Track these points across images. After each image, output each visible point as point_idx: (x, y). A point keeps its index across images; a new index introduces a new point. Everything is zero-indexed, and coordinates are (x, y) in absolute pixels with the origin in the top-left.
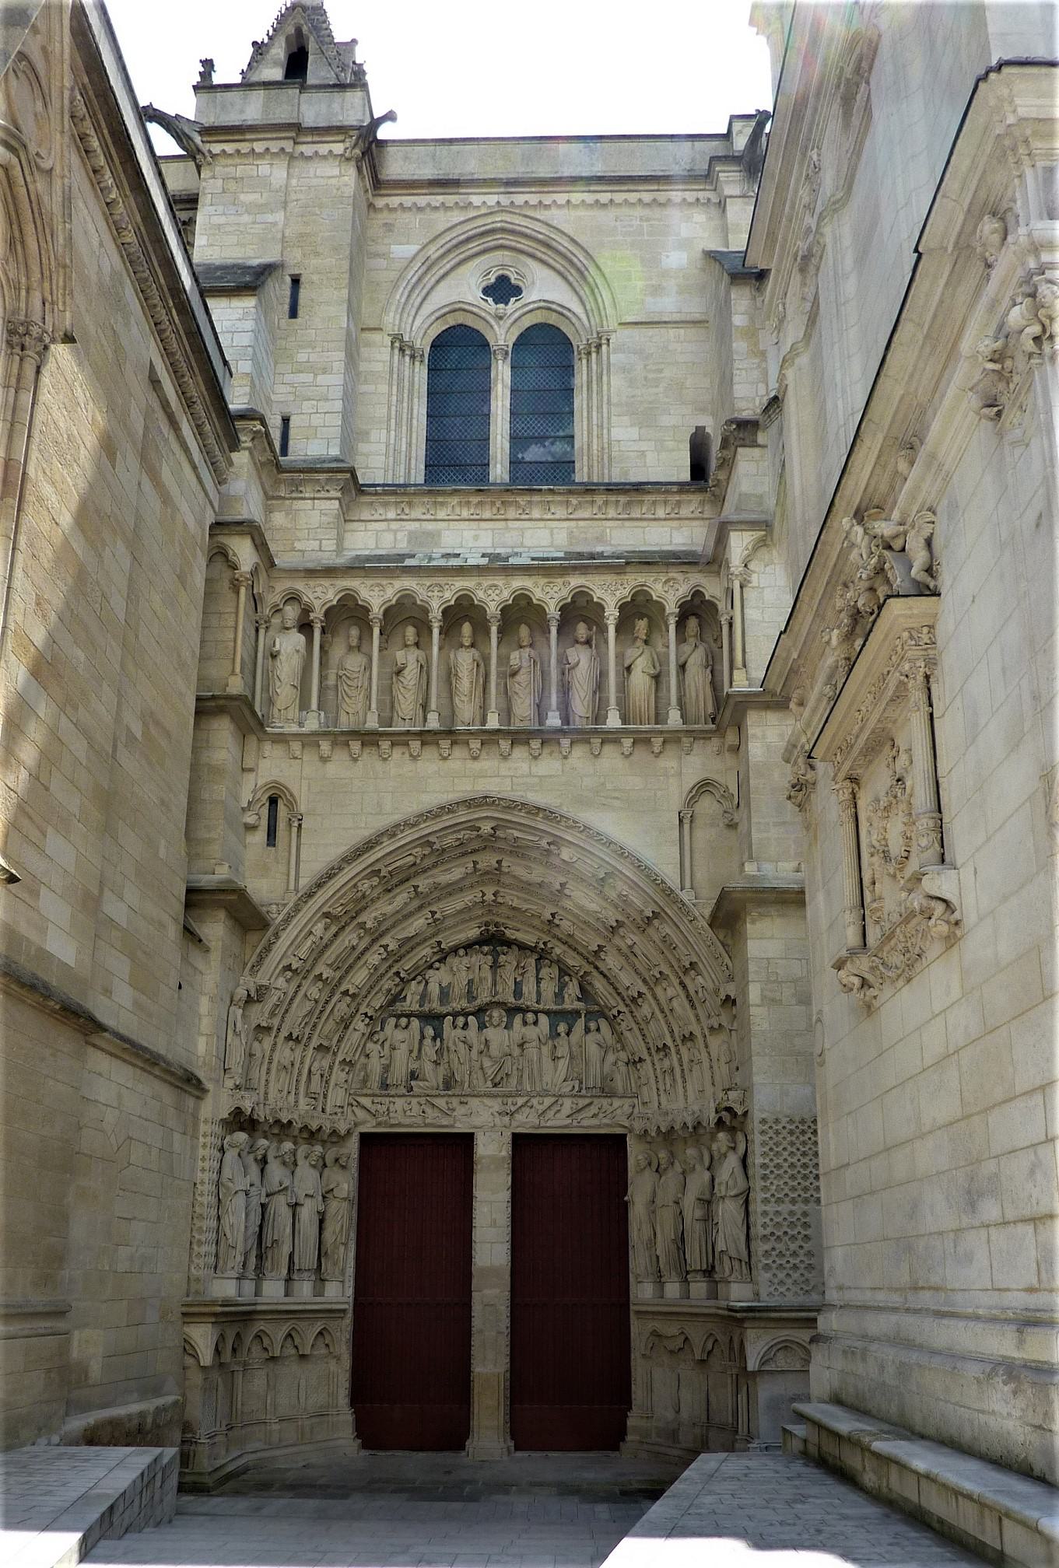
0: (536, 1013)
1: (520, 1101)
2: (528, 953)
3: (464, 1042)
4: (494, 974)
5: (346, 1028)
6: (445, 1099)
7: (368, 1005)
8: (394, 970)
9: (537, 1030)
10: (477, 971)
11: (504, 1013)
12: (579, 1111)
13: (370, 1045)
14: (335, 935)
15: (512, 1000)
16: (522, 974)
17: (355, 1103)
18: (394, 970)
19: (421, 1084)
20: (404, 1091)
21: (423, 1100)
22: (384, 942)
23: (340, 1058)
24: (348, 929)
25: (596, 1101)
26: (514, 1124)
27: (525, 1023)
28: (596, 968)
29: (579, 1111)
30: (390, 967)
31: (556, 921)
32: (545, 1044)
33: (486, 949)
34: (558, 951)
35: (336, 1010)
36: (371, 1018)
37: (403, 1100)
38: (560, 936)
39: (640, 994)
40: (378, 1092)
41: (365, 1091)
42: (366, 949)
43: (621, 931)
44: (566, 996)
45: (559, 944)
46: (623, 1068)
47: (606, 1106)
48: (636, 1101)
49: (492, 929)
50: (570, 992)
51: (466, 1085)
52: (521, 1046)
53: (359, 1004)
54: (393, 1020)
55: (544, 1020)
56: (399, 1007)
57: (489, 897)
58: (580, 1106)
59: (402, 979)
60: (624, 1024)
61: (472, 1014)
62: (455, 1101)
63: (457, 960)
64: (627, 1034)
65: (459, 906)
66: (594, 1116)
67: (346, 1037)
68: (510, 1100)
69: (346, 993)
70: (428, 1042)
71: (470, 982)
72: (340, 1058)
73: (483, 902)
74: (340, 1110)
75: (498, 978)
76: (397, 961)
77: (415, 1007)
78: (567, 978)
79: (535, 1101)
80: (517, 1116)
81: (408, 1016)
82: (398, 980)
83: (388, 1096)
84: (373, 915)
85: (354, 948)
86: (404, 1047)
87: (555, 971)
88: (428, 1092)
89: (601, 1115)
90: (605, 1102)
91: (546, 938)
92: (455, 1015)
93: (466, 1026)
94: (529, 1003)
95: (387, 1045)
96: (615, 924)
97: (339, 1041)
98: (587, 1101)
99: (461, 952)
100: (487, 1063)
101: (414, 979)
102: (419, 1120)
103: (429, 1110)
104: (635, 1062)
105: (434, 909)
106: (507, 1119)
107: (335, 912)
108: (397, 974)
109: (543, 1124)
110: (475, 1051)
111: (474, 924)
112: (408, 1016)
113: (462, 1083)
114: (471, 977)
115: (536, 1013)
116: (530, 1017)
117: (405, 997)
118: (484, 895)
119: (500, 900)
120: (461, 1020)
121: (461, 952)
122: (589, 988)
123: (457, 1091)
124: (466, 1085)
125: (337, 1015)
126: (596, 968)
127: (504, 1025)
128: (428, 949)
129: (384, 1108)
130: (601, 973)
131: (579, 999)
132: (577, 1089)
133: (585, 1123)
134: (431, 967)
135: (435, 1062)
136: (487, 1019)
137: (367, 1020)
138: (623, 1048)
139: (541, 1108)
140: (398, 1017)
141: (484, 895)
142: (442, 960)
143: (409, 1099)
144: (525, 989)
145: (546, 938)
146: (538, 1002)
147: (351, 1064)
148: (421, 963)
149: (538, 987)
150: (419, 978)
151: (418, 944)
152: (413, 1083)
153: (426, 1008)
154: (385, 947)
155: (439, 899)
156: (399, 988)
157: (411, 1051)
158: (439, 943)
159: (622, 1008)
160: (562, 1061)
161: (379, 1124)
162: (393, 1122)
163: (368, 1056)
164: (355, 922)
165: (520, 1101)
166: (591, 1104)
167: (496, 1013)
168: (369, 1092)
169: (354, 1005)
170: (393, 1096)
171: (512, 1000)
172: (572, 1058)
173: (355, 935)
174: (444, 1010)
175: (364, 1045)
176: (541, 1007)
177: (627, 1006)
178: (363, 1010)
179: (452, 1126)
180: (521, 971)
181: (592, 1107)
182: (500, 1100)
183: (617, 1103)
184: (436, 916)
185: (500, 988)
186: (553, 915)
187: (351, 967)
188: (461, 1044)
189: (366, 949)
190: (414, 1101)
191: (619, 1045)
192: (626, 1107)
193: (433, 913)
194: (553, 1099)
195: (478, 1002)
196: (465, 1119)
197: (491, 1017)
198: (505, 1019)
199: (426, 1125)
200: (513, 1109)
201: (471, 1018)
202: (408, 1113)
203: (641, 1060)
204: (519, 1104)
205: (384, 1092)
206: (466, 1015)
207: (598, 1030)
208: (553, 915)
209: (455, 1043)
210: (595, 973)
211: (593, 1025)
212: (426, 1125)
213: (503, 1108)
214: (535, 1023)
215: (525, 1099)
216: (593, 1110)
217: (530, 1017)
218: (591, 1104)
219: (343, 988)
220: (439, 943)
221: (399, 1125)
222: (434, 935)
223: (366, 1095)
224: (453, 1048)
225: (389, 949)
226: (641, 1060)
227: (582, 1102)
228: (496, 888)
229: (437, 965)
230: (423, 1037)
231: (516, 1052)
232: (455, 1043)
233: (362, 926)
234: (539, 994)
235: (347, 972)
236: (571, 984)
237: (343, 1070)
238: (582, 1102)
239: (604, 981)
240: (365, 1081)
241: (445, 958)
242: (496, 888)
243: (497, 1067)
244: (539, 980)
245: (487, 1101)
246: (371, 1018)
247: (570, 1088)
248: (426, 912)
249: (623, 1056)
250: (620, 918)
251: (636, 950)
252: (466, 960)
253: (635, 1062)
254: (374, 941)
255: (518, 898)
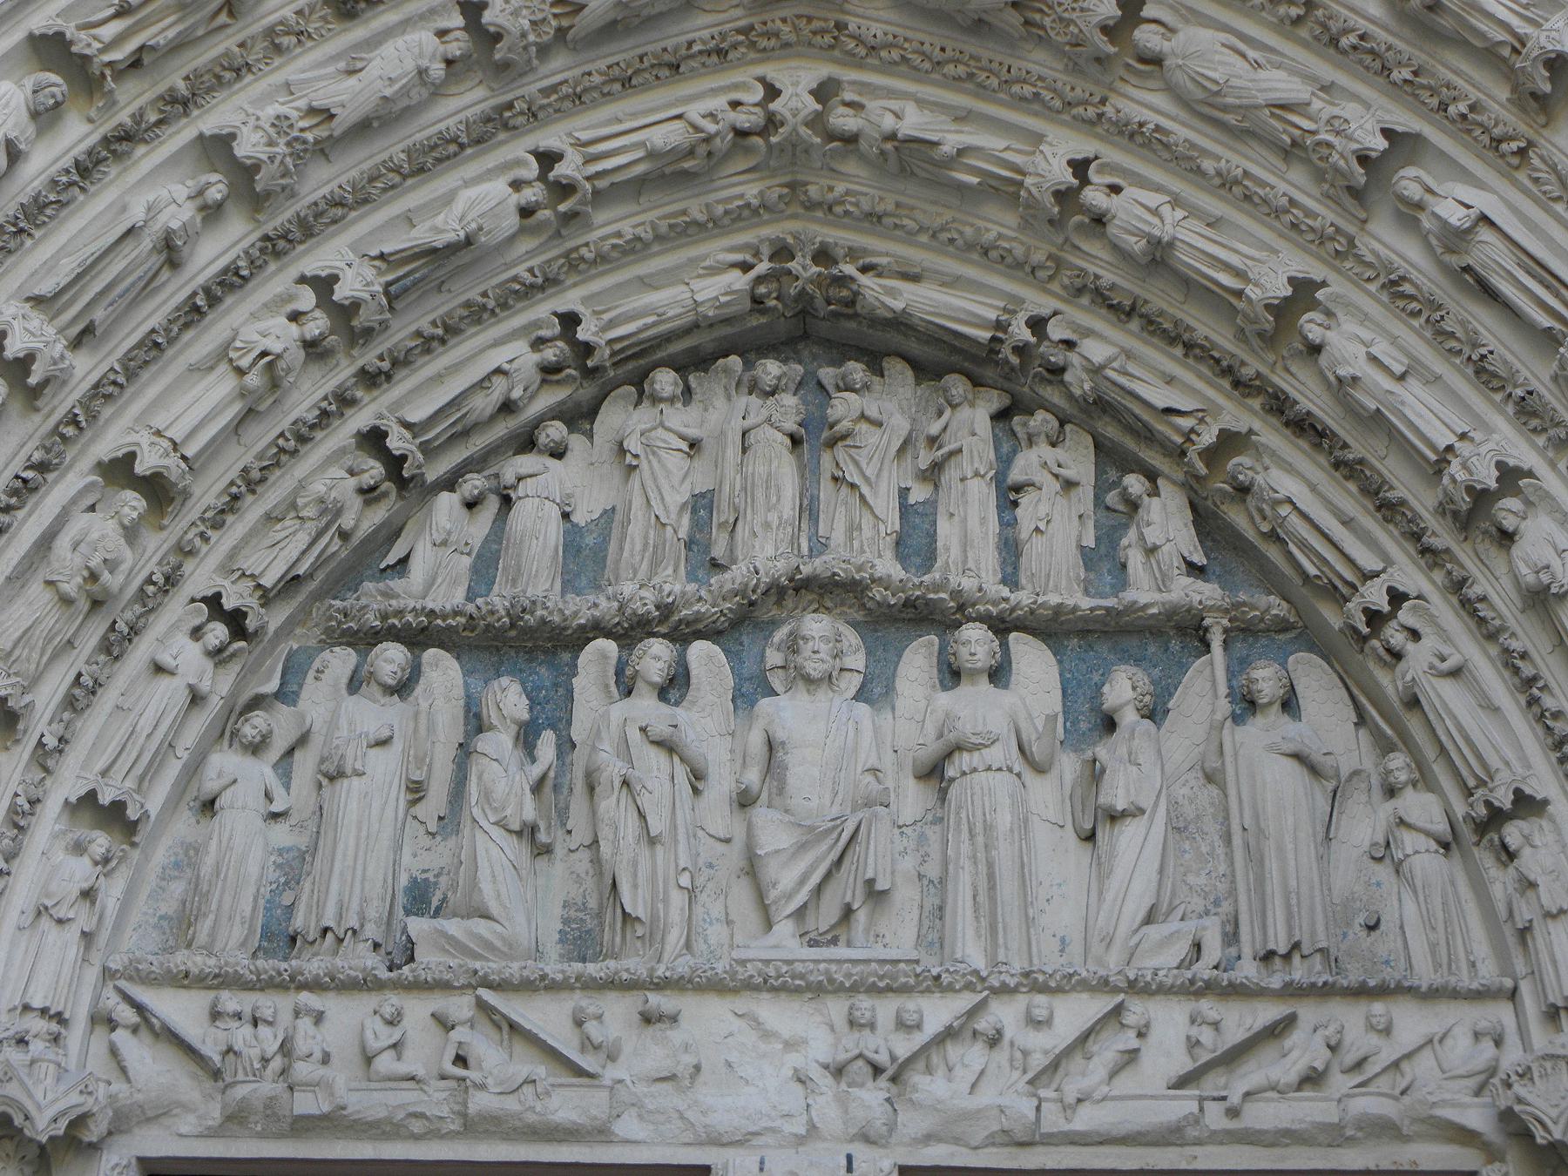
0: (1001, 626)
1: (938, 1013)
2: (957, 385)
3: (668, 746)
4: (808, 473)
5: (114, 647)
6: (578, 999)
7: (226, 568)
8: (361, 419)
9: (1005, 698)
10: (732, 452)
11: (851, 637)
12: (1233, 1057)
13: (225, 762)
14: (86, 169)
15: (888, 567)
16: (933, 473)
17: (127, 1014)
18: (361, 419)
19: (453, 927)
20: (374, 963)
21: (460, 1006)
22: (319, 258)
23: (68, 784)
24: (147, 159)
25: (1308, 1013)
26: (912, 1123)
27: (952, 674)
28: (1278, 405)
29: (1233, 1057)
30: (344, 401)
31: (1094, 196)
32: (1040, 769)
33: (771, 369)
34: (1096, 351)
35: (63, 543)
36: (236, 621)
37: (369, 1001)
38: (1108, 277)
39: (1510, 476)
40: (241, 962)
41: (182, 960)
42: (232, 281)
43: (1409, 180)
44: (1135, 559)
45: (1097, 322)
46: (1426, 862)
47: (1358, 1040)
48: (1503, 1013)
49: (804, 268)
50: (1153, 535)
51: (675, 938)
52: (934, 772)
53: (185, 551)
54: (341, 661)
55: (1031, 658)
56: (370, 601)
57: (797, 100)
58: (1235, 1034)
59: (394, 464)
60: (1419, 657)
61: (713, 634)
62: (616, 1013)
63: (644, 416)
64: (1448, 697)
65: (667, 136)
66: (1312, 1079)
67: (108, 699)
68: (885, 1009)
69: (120, 470)
70: (499, 743)
71: (702, 504)
72: (68, 784)
73: (772, 123)
74: (38, 1025)
75: (826, 489)
76: (371, 379)
77: (449, 596)
78: (1135, 484)
79: (1006, 1014)
80: (930, 1086)
81: (418, 637)
82: (374, 470)
83: (298, 983)
84: (272, 110)
85: (171, 252)
86: (384, 768)
87: (1079, 461)
88: (491, 967)
89: (1340, 1083)
90: (1350, 1019)
91: (1040, 303)
92: (631, 632)
93: (675, 685)
94: (968, 584)
95: (306, 764)
96: (1381, 144)
97: (70, 703)
98: (1268, 1013)
99: (665, 381)
100: (773, 834)
101: (449, 483)
102: (436, 1101)
103: (487, 1050)
104: (1496, 817)
105: (549, 139)
106: (871, 1097)
107: (84, 43)
108: (374, 439)
109: (1053, 1121)
110: (720, 786)
111: (718, 249)
112: (418, 637)
113: (654, 935)
114: (702, 485)
115: (1001, 626)
116: (975, 641)
117: (404, 561)
118: (772, 92)
119: (844, 120)
120: (655, 656)
121: (665, 381)
122: (1237, 517)
123: (633, 964)
124: (675, 938)
125: (66, 563)
126: (1278, 405)
127: (852, 683)
128: (520, 347)
129: (269, 1040)
130: (1304, 427)
131: (1194, 570)
132: (1214, 950)
133: (1266, 1115)
134: (526, 442)
135: (528, 832)
136: (774, 657)
137: (218, 632)
138: (1423, 779)
139: (1044, 1043)
140: (365, 640)
141: (772, 92)
142: (581, 416)
143: (392, 1001)
144: (946, 530)
145: (1040, 303)
146: (1010, 580)
147: (115, 818)
148: (484, 404)
149: (1008, 523)
150: (474, 484)
151: (478, 314)
152: (418, 926)
153: (498, 599)
154: (323, 285)
155: (579, 99)
156: (378, 515)
157: (416, 791)
158: (570, 321)
159: (1409, 575)
160: (1130, 831)
161: (236, 1118)
162: (305, 1104)
163: (209, 806)
164: (181, 135)
165: (938, 1013)
166: (1276, 1031)
167: (816, 625)
168: (197, 962)
169: (156, 544)
170: (315, 986)
171: (888, 567)
172: (1178, 828)
173: (181, 192)
174: (581, 608)
175: (195, 767)
176: (1024, 598)
177: (1431, 556)
178: (201, 578)
179: (601, 1133)
180: (925, 459)
181: (1296, 1037)
182: (837, 1008)
183: (1412, 1023)
184: (561, 170)
185: (835, 525)
186: (1080, 167)
187: (153, 347)
188: (656, 760)
189: (232, 281)
190: (417, 1010)
191: (1398, 761)
192: (1461, 1043)
193: (548, 159)
194: (1099, 1005)
195: (737, 574)
196: (666, 1097)
197: (793, 645)
198: (857, 661)
199: (472, 1127)
200: (904, 1047)
201: (701, 652)
202: (385, 1063)
203: (1527, 805)
204: (933, 1026)
205: (267, 965)
206: (683, 634)
207: (1289, 704)
208: (1080, 167)
209: (624, 745)
210: (1270, 435)
211: (1266, 679)
212: (472, 1127)
213: (852, 1043)
214: (998, 674)
215: (966, 1001)
216: (1303, 1050)
217: (975, 641)
218: (1276, 1031)
219: (107, 445)
220: (570, 321)
221: (333, 1122)
222: (550, 283)
223: (183, 980)
224: (613, 768)
225: (341, 293)
226: (1527, 805)
227: (1241, 1020)
228: (824, 70)
229: (555, 431)
230: (476, 723)
231: (912, 799)
232: (624, 745)
233: (217, 148)
234: (1011, 549)
235: (134, 367)
236: (1154, 509)
237: (79, 848)
238: (1241, 1020)
239: (1313, 467)
240: (182, 925)
241: (592, 412)
242: (824, 70)
243: (822, 855)
244: (1009, 495)
245: (778, 1014)
246: (236, 621)
247: (1182, 949)
248: (518, 150)
249: (1421, 807)
250: (1405, 120)
251: (1489, 253)
252: (682, 419)
253: (1496, 817)
254: (274, 247)
255: (921, 103)
